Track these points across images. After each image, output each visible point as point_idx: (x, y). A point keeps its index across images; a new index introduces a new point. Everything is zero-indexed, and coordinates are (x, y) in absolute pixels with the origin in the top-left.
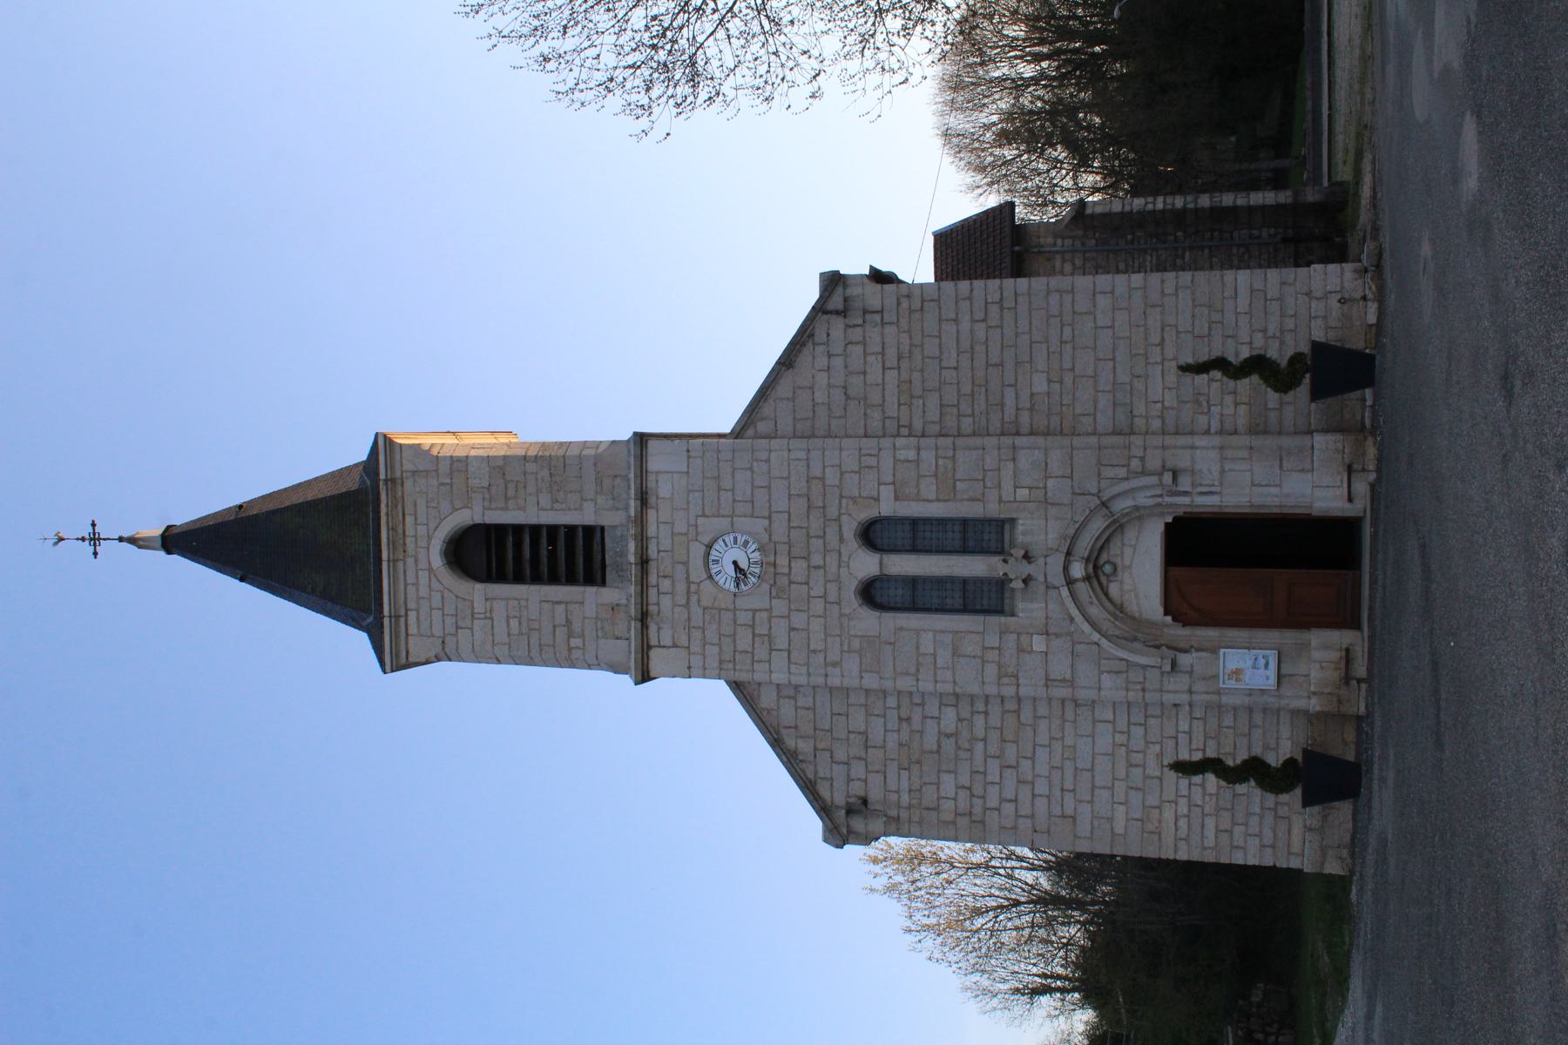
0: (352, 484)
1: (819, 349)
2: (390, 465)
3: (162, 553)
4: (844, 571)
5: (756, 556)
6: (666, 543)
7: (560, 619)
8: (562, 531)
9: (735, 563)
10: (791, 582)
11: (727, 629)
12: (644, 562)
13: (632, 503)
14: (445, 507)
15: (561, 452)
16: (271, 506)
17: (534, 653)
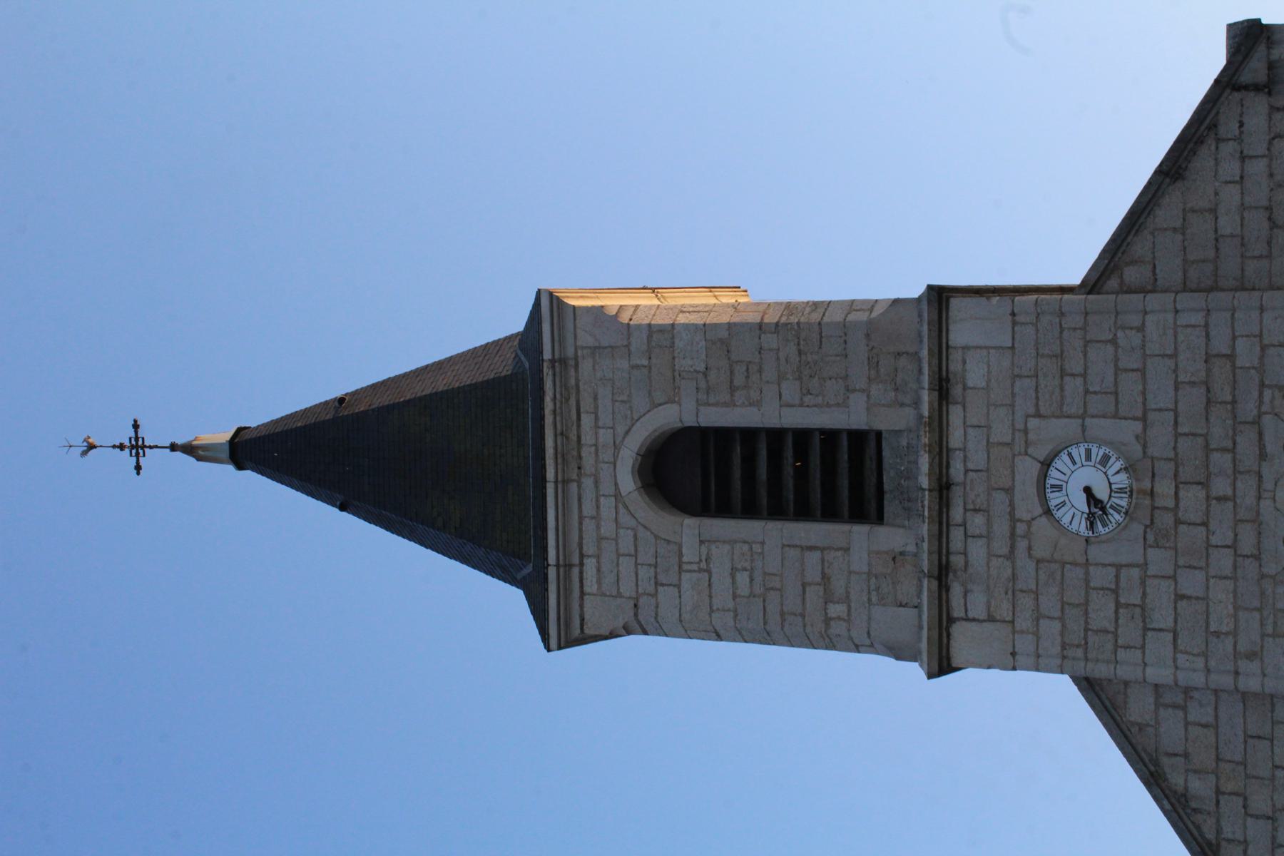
0: (502, 367)
1: (1228, 148)
3: (230, 468)
4: (1266, 504)
5: (1122, 480)
6: (978, 459)
7: (813, 574)
8: (816, 440)
9: (1088, 490)
10: (1178, 522)
12: (943, 487)
13: (925, 396)
15: (816, 317)
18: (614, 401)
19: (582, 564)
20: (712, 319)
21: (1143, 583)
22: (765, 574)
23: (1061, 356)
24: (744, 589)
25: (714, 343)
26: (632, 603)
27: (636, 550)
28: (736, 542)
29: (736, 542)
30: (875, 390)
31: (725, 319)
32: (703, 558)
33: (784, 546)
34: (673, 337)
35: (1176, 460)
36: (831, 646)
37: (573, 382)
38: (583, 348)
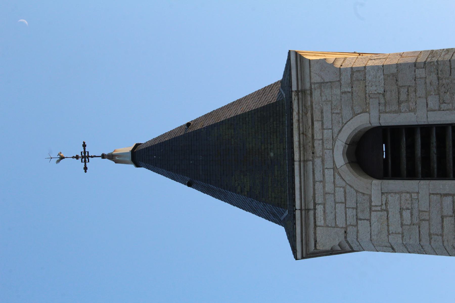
0: (272, 98)
2: (301, 78)
3: (132, 166)
14: (347, 113)
15: (448, 57)
16: (211, 122)
18: (332, 113)
19: (315, 209)
22: (420, 211)
24: (407, 221)
25: (388, 76)
26: (343, 231)
27: (345, 200)
28: (402, 192)
29: (402, 192)
31: (395, 62)
32: (384, 203)
33: (430, 194)
34: (365, 74)
37: (309, 103)
38: (315, 83)
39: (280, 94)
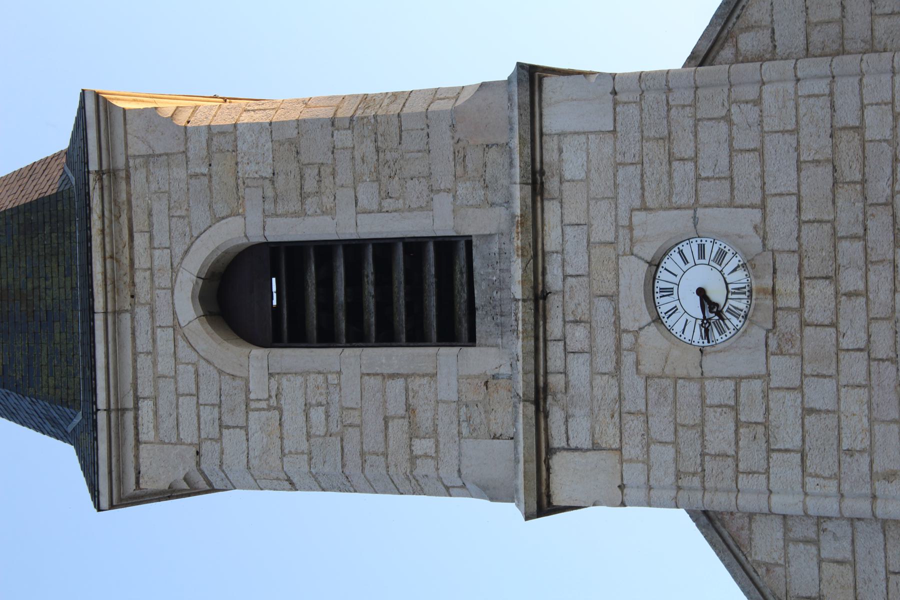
0: (48, 186)
2: (106, 146)
5: (739, 278)
6: (577, 262)
7: (396, 407)
9: (701, 292)
10: (804, 324)
11: (689, 415)
12: (539, 297)
14: (200, 215)
15: (395, 109)
17: (353, 468)
18: (171, 217)
19: (136, 408)
20: (279, 117)
21: (766, 396)
22: (343, 408)
23: (669, 138)
24: (319, 427)
25: (282, 144)
26: (193, 451)
27: (198, 388)
28: (309, 373)
29: (309, 373)
30: (463, 189)
31: (293, 116)
32: (273, 393)
33: (363, 375)
34: (235, 140)
35: (799, 253)
36: (419, 490)
37: (123, 197)
38: (135, 157)
39: (65, 179)
